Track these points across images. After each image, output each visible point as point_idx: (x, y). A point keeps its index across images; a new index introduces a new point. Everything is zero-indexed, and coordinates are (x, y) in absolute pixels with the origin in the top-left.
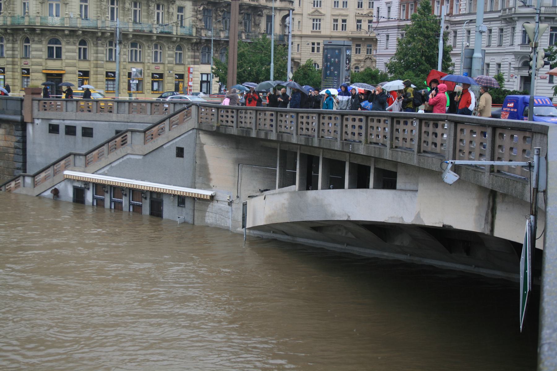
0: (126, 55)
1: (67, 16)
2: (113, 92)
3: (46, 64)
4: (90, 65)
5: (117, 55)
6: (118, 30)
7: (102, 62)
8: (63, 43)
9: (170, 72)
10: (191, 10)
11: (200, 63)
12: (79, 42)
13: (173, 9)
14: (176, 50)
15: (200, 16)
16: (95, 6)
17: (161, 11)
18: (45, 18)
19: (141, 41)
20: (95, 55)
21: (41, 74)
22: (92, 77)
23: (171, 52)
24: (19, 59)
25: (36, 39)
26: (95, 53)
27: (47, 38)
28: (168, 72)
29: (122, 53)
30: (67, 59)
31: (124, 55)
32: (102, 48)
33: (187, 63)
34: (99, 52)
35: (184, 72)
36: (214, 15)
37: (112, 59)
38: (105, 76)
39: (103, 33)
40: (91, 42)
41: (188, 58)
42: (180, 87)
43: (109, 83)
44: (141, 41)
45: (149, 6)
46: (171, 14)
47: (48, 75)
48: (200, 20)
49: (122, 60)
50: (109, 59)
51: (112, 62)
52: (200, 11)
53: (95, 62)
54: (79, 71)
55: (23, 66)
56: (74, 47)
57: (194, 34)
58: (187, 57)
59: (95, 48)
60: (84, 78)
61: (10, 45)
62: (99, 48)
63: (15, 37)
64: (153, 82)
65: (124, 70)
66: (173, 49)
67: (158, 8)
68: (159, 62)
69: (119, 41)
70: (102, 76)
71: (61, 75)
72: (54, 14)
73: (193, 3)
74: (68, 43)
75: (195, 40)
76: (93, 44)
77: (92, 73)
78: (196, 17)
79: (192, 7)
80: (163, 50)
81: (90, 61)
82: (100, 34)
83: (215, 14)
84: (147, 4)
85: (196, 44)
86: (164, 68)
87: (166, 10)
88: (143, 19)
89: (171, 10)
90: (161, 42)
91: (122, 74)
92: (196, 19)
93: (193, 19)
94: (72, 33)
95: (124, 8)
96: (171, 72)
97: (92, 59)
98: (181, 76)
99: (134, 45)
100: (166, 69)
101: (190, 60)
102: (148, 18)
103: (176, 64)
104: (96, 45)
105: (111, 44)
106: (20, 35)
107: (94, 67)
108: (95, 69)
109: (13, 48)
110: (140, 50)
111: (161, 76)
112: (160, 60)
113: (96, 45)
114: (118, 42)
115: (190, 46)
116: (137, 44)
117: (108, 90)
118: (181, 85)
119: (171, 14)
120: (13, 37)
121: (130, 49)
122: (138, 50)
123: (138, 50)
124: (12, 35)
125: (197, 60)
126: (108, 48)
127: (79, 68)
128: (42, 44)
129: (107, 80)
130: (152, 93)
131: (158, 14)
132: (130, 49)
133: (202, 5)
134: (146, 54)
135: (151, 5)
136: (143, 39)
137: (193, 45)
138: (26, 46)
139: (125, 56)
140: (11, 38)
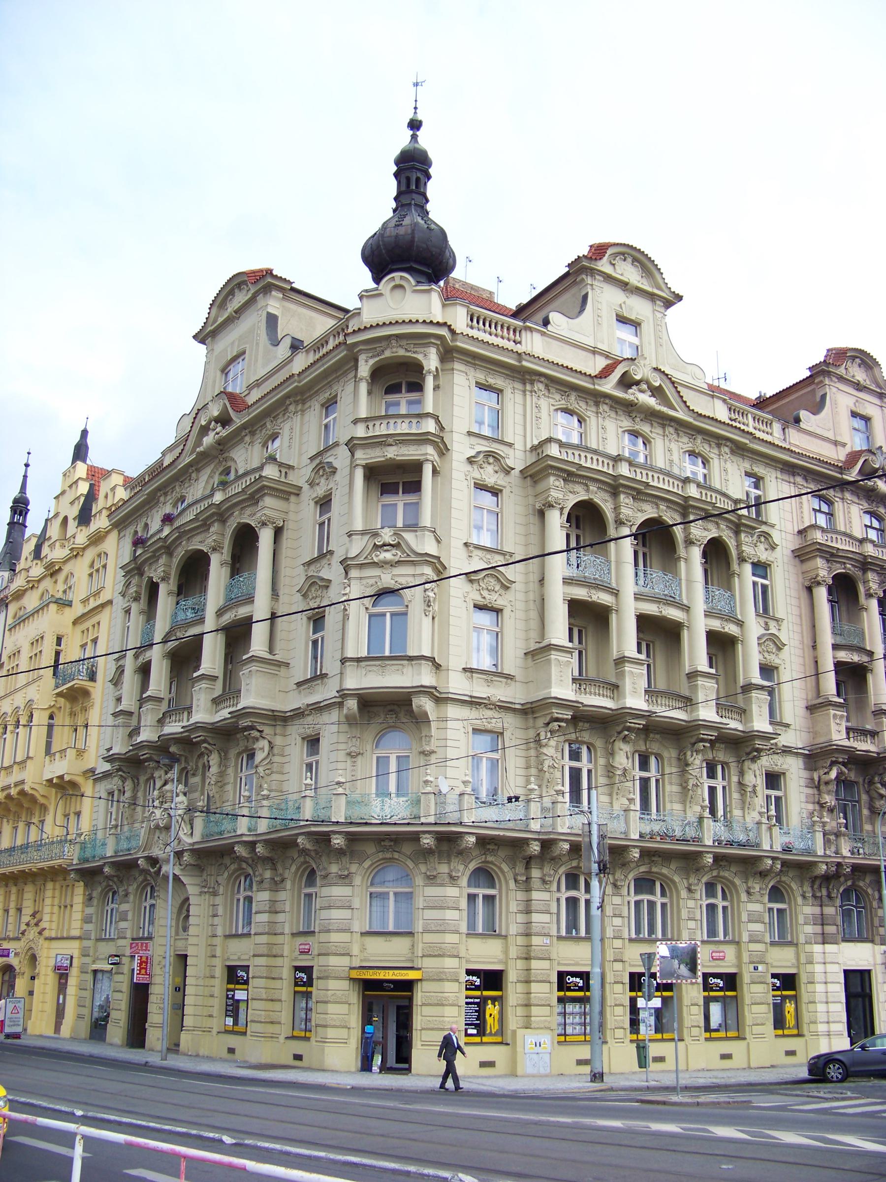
0: (620, 916)
1: (429, 789)
2: (582, 1038)
3: (363, 949)
4: (506, 951)
5: (595, 912)
6: (595, 829)
7: (547, 940)
8: (419, 881)
9: (756, 968)
10: (803, 782)
11: (840, 937)
12: (468, 873)
13: (755, 777)
14: (770, 901)
15: (829, 799)
16: (521, 762)
17: (719, 783)
18: (363, 802)
19: (665, 871)
20: (520, 918)
21: (345, 984)
22: (513, 991)
23: (752, 907)
24: (287, 938)
25: (334, 869)
26: (521, 912)
27: (367, 864)
28: (751, 967)
29: (609, 910)
30: (426, 931)
31: (615, 916)
32: (545, 896)
33: (802, 939)
34: (535, 905)
35: (798, 967)
36: (864, 797)
37: (577, 931)
38: (555, 986)
39: (547, 844)
40: (510, 875)
41: (806, 924)
42: (788, 1016)
43: (570, 1008)
44: (665, 871)
45: (687, 765)
46: (749, 789)
47: (368, 986)
48: (831, 810)
49: (609, 933)
50: (568, 931)
51: (579, 939)
52: (827, 783)
53: (520, 940)
54: (469, 972)
55: (296, 959)
56: (452, 891)
57: (820, 852)
58: (801, 920)
59: (521, 895)
60: (486, 993)
61: (264, 896)
62: (535, 895)
63: (280, 871)
64: (707, 1001)
65: (618, 966)
66: (762, 895)
67: (712, 774)
68: (721, 937)
69: (599, 863)
70: (545, 987)
71: (408, 986)
72: (392, 788)
73: (805, 763)
74: (431, 879)
75: (824, 867)
76: (516, 881)
77: (512, 976)
78: (818, 803)
79: (805, 774)
80: (732, 901)
81: (505, 937)
82: (535, 848)
83: (868, 792)
84: (679, 759)
85: (827, 879)
86: (739, 956)
87: (735, 779)
88: (668, 806)
89: (749, 779)
90: (726, 874)
91: (609, 978)
92: (817, 807)
93: (810, 807)
94: (445, 847)
95: (610, 770)
96: (761, 967)
97: (513, 929)
98: (788, 982)
99: (644, 884)
100: (745, 958)
101: (809, 929)
102: (683, 802)
103: (773, 944)
104: (527, 886)
105: (572, 880)
106: (293, 860)
107: (518, 958)
108: (520, 964)
109: (273, 902)
110: (665, 900)
111: (731, 981)
112: (726, 934)
113: (527, 886)
114: (595, 867)
115: (807, 888)
116: (654, 881)
117: (565, 1035)
118: (789, 1007)
119: (749, 789)
120: (274, 869)
121: (633, 898)
122: (658, 899)
123: (658, 899)
124: (270, 862)
125: (830, 929)
126: (565, 894)
127: (468, 961)
128: (350, 884)
129: (561, 1000)
130: (706, 1039)
131: (712, 790)
132: (633, 898)
133: (833, 763)
134: (684, 914)
135: (690, 760)
136: (673, 866)
137: (817, 883)
138: (309, 896)
139: (617, 921)
140: (268, 874)
